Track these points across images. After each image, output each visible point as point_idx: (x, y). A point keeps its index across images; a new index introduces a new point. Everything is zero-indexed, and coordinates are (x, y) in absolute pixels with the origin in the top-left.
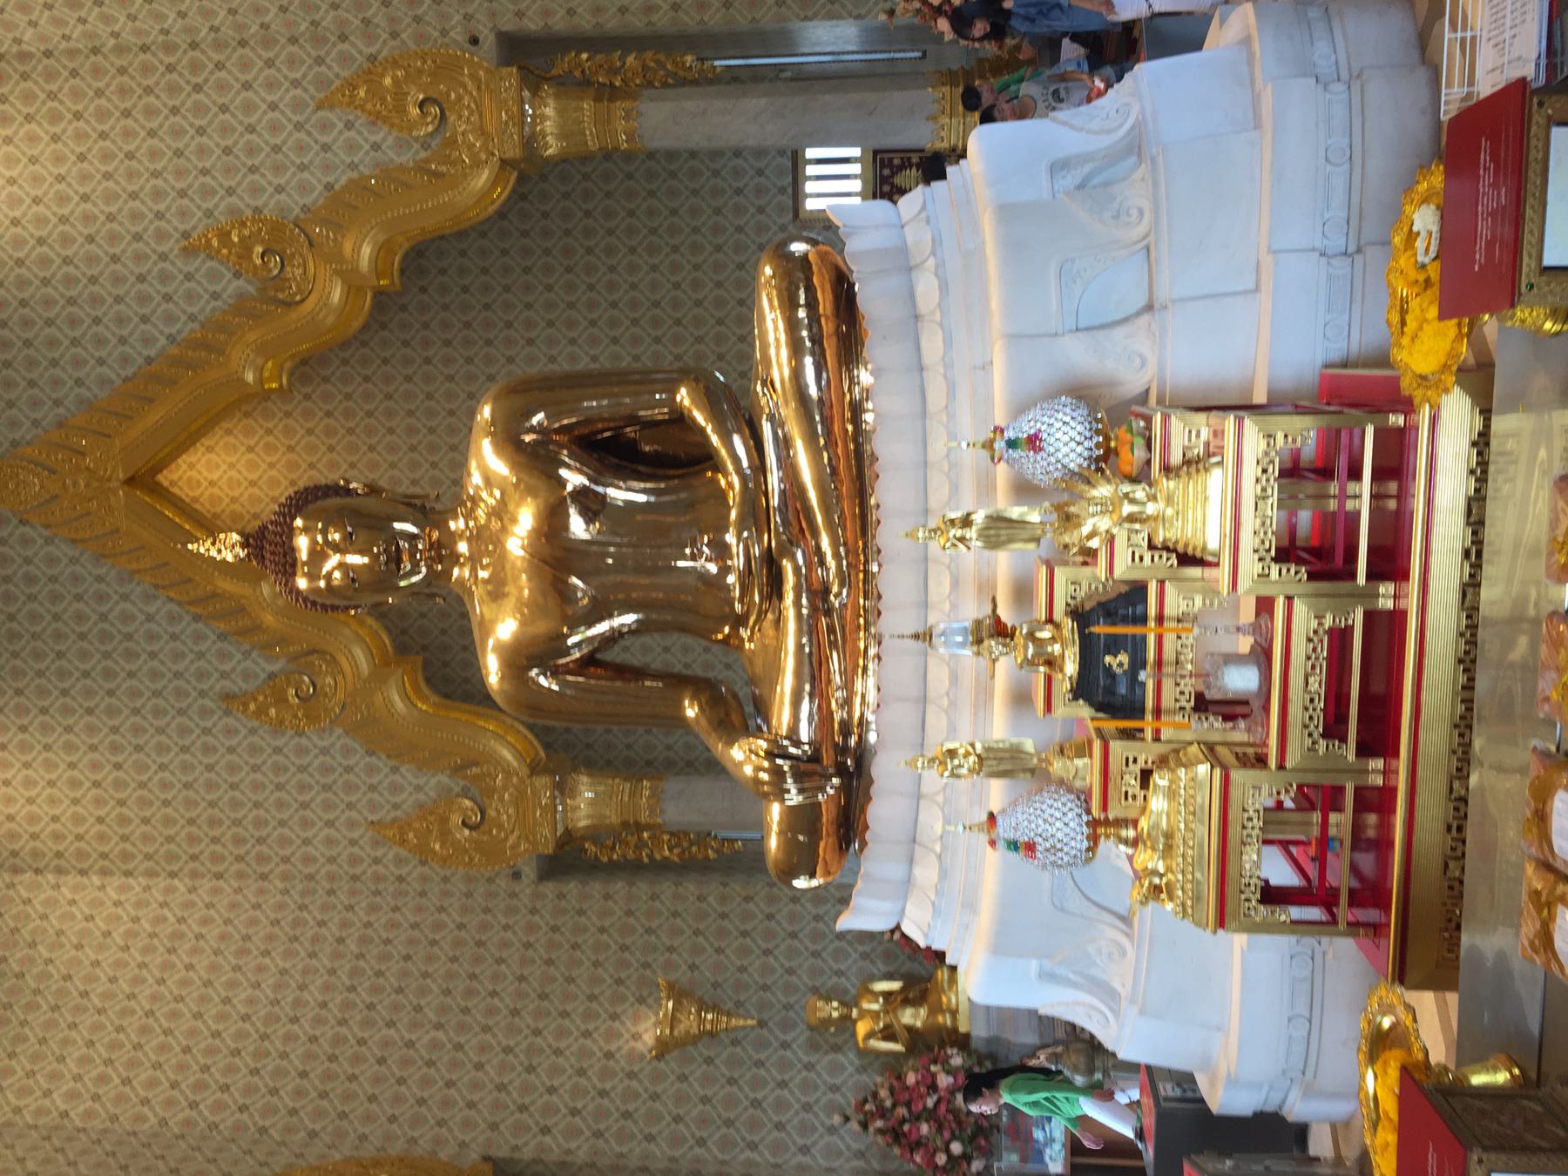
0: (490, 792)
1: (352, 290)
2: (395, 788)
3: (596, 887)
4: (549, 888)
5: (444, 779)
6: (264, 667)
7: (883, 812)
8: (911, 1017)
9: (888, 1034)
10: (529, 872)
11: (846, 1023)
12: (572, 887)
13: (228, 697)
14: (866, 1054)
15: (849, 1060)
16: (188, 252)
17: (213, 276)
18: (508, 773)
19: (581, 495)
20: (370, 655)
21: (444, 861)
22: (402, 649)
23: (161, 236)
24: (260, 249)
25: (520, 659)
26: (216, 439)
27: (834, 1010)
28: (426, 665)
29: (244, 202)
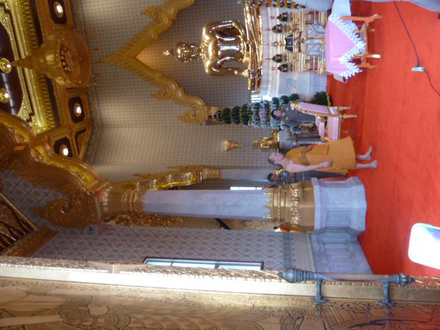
0: (196, 110)
1: (169, 20)
2: (180, 110)
3: (215, 126)
4: (207, 127)
5: (188, 108)
6: (157, 89)
7: (264, 78)
8: (270, 142)
9: (266, 145)
10: (204, 124)
11: (259, 144)
12: (211, 126)
13: (152, 95)
14: (262, 149)
15: (260, 150)
16: (141, 14)
17: (146, 19)
18: (200, 106)
19: (220, 39)
20: (175, 86)
21: (189, 122)
22: (180, 86)
23: (137, 12)
24: (153, 13)
25: (210, 67)
26: (143, 52)
27: (256, 142)
28: (184, 89)
29: (150, 5)
